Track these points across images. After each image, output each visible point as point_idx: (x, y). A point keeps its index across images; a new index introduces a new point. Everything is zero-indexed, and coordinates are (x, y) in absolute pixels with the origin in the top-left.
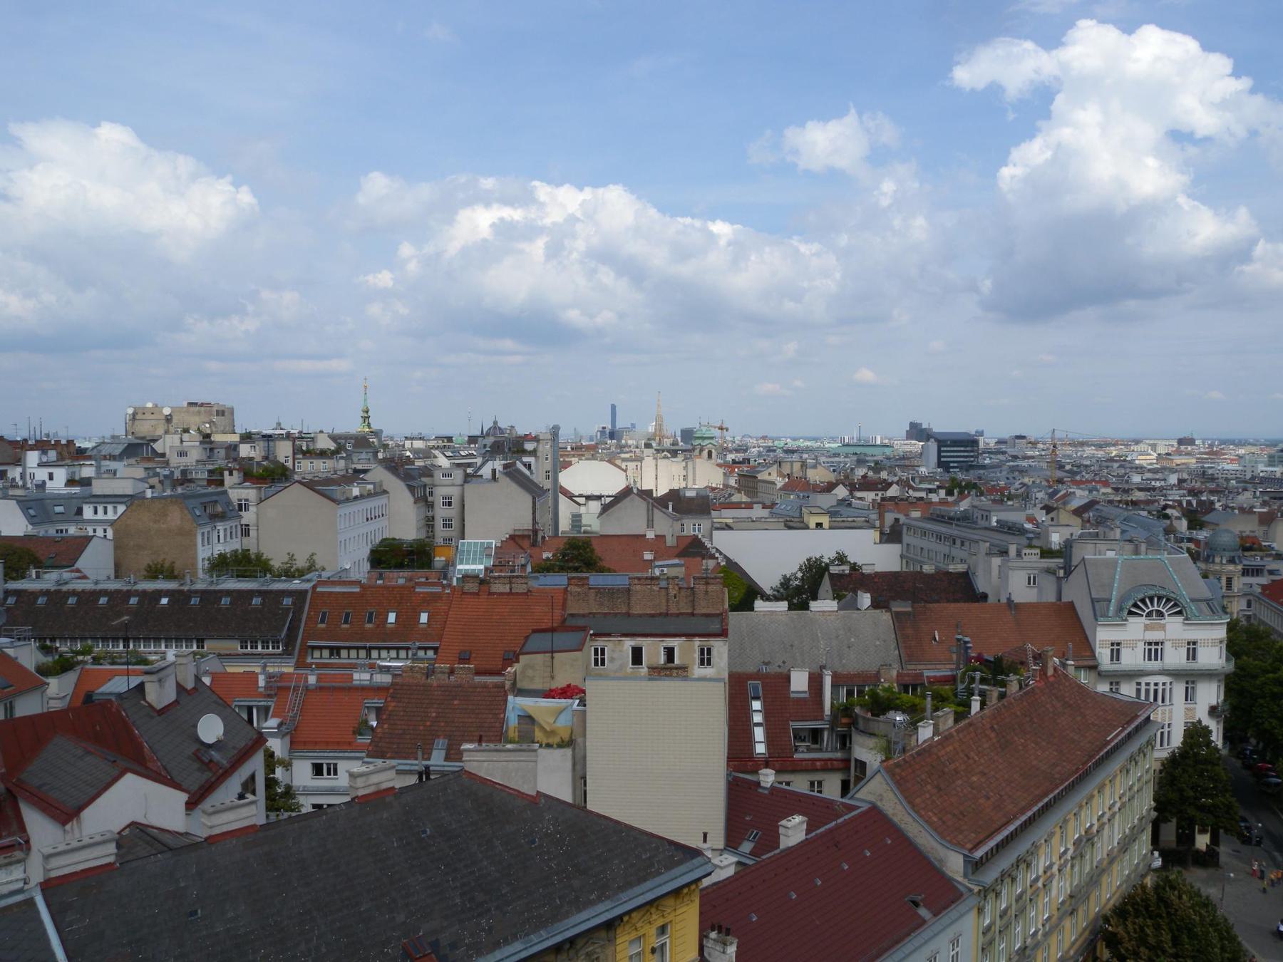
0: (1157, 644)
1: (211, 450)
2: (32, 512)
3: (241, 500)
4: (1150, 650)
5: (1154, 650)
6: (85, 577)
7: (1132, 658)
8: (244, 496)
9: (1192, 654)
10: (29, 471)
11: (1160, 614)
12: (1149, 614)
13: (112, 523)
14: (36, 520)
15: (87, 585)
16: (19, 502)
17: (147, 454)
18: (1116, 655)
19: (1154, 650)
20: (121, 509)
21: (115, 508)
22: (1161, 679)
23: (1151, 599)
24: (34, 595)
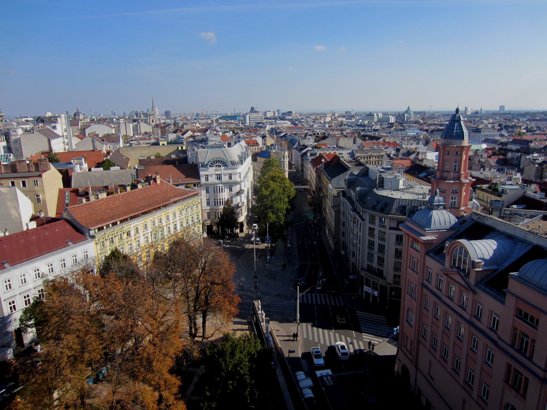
0: (219, 175)
4: (217, 177)
5: (219, 177)
7: (213, 179)
9: (230, 178)
11: (220, 166)
12: (216, 166)
18: (207, 179)
19: (219, 177)
22: (221, 185)
23: (216, 162)
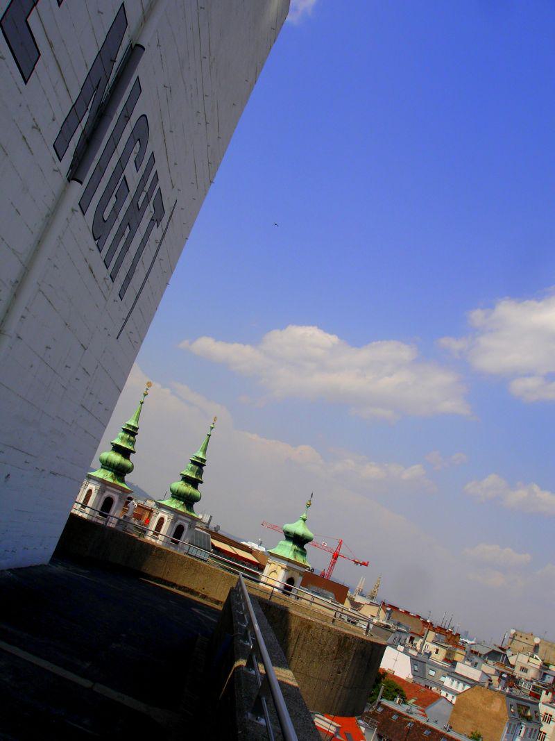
1: (545, 674)
2: (416, 668)
3: (546, 714)
6: (425, 716)
8: (550, 712)
10: (426, 643)
13: (458, 694)
14: (416, 673)
15: (423, 721)
16: (411, 658)
17: (502, 661)
20: (467, 687)
21: (464, 685)
24: (393, 712)
